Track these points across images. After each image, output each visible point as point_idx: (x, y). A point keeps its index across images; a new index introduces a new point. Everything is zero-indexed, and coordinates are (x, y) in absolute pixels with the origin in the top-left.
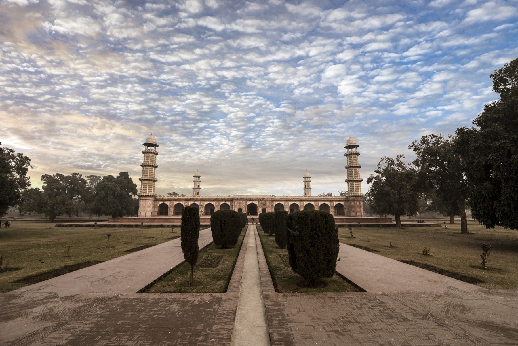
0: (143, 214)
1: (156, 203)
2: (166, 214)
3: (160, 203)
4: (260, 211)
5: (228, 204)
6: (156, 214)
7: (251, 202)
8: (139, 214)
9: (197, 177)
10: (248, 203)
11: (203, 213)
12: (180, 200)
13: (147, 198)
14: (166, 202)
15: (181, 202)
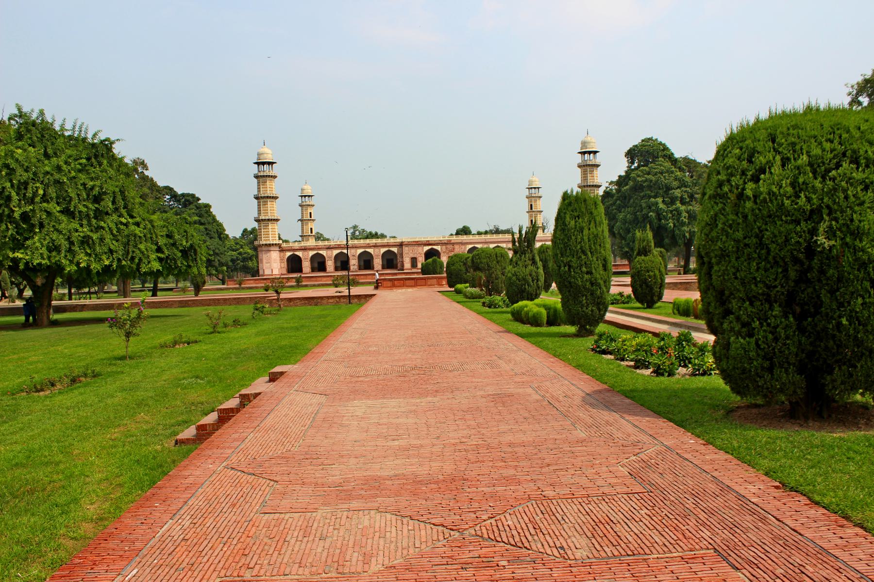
0: (267, 272)
1: (282, 254)
2: (300, 270)
3: (289, 254)
4: (444, 259)
5: (393, 252)
6: (285, 272)
7: (430, 247)
8: (261, 272)
9: (305, 196)
10: (427, 248)
11: (356, 267)
12: (319, 249)
13: (272, 248)
14: (297, 253)
15: (321, 252)
